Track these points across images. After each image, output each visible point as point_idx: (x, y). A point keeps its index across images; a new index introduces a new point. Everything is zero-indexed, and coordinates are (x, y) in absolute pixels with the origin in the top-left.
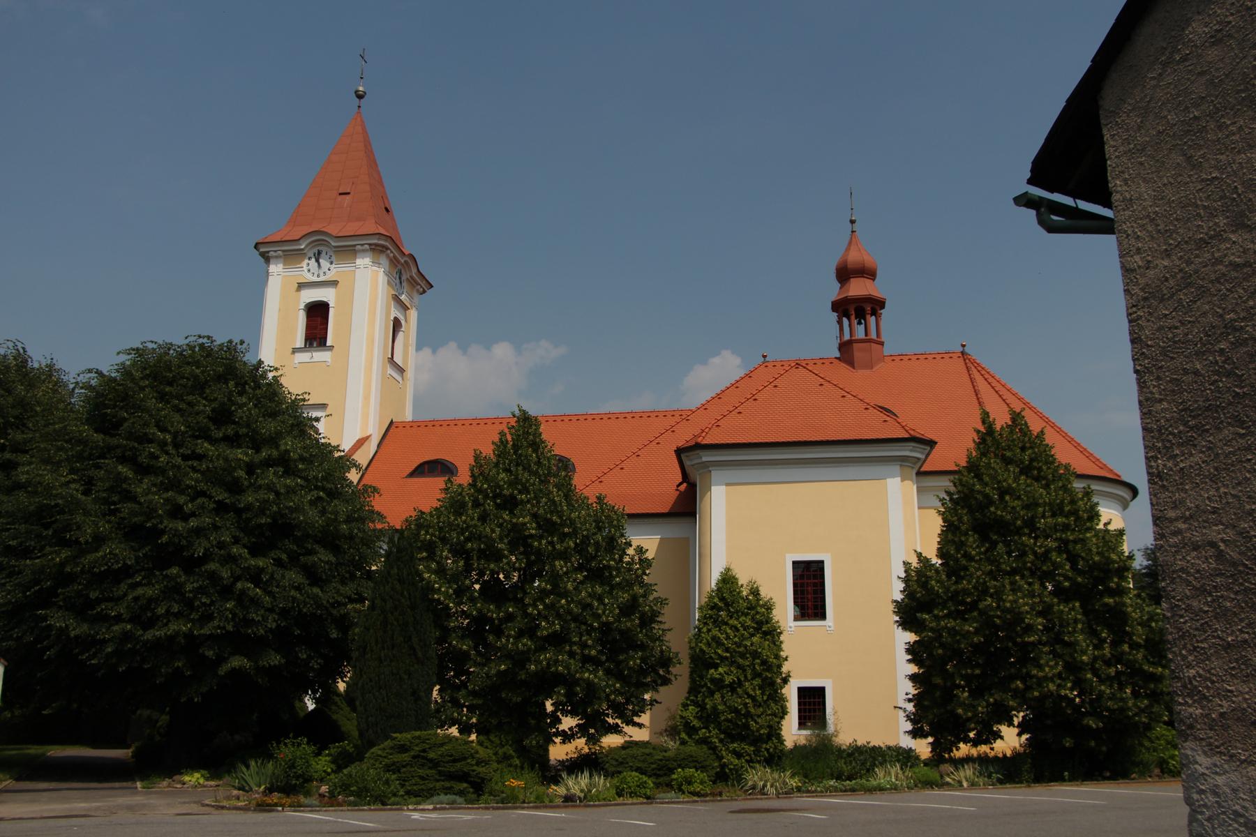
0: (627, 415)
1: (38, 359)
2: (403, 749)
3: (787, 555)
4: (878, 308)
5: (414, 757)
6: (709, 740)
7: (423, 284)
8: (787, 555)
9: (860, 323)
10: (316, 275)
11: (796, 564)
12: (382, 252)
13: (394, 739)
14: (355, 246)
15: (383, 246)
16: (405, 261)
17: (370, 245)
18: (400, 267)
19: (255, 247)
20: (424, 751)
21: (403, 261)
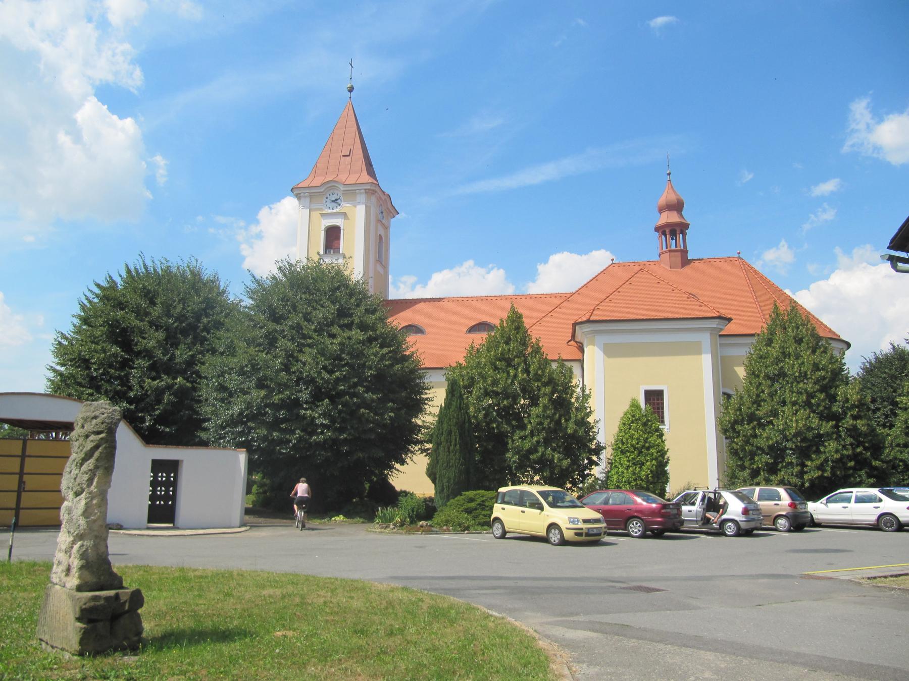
0: (542, 296)
1: (207, 275)
2: (471, 500)
3: (641, 386)
4: (684, 229)
5: (478, 504)
6: (655, 473)
7: (392, 211)
8: (641, 386)
9: (672, 239)
10: (331, 208)
11: (662, 391)
12: (372, 194)
13: (465, 495)
14: (356, 190)
15: (373, 190)
16: (385, 199)
17: (365, 189)
18: (381, 202)
19: (291, 190)
20: (483, 501)
21: (383, 199)
